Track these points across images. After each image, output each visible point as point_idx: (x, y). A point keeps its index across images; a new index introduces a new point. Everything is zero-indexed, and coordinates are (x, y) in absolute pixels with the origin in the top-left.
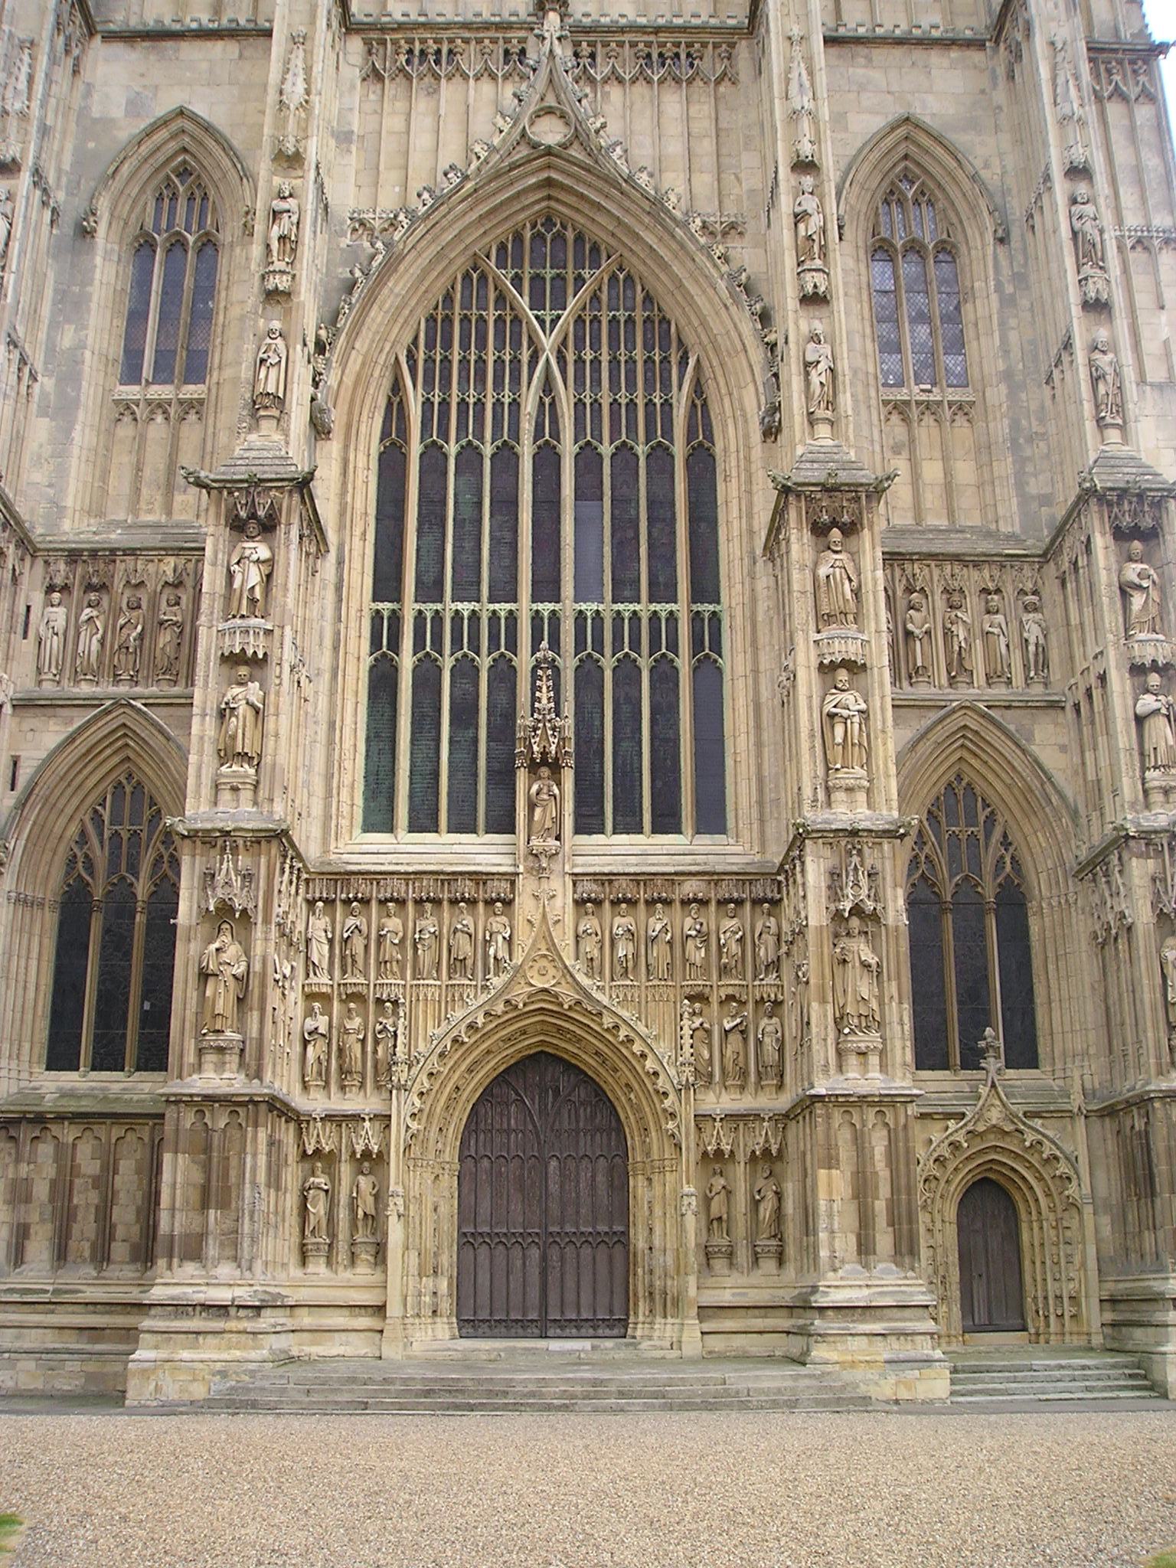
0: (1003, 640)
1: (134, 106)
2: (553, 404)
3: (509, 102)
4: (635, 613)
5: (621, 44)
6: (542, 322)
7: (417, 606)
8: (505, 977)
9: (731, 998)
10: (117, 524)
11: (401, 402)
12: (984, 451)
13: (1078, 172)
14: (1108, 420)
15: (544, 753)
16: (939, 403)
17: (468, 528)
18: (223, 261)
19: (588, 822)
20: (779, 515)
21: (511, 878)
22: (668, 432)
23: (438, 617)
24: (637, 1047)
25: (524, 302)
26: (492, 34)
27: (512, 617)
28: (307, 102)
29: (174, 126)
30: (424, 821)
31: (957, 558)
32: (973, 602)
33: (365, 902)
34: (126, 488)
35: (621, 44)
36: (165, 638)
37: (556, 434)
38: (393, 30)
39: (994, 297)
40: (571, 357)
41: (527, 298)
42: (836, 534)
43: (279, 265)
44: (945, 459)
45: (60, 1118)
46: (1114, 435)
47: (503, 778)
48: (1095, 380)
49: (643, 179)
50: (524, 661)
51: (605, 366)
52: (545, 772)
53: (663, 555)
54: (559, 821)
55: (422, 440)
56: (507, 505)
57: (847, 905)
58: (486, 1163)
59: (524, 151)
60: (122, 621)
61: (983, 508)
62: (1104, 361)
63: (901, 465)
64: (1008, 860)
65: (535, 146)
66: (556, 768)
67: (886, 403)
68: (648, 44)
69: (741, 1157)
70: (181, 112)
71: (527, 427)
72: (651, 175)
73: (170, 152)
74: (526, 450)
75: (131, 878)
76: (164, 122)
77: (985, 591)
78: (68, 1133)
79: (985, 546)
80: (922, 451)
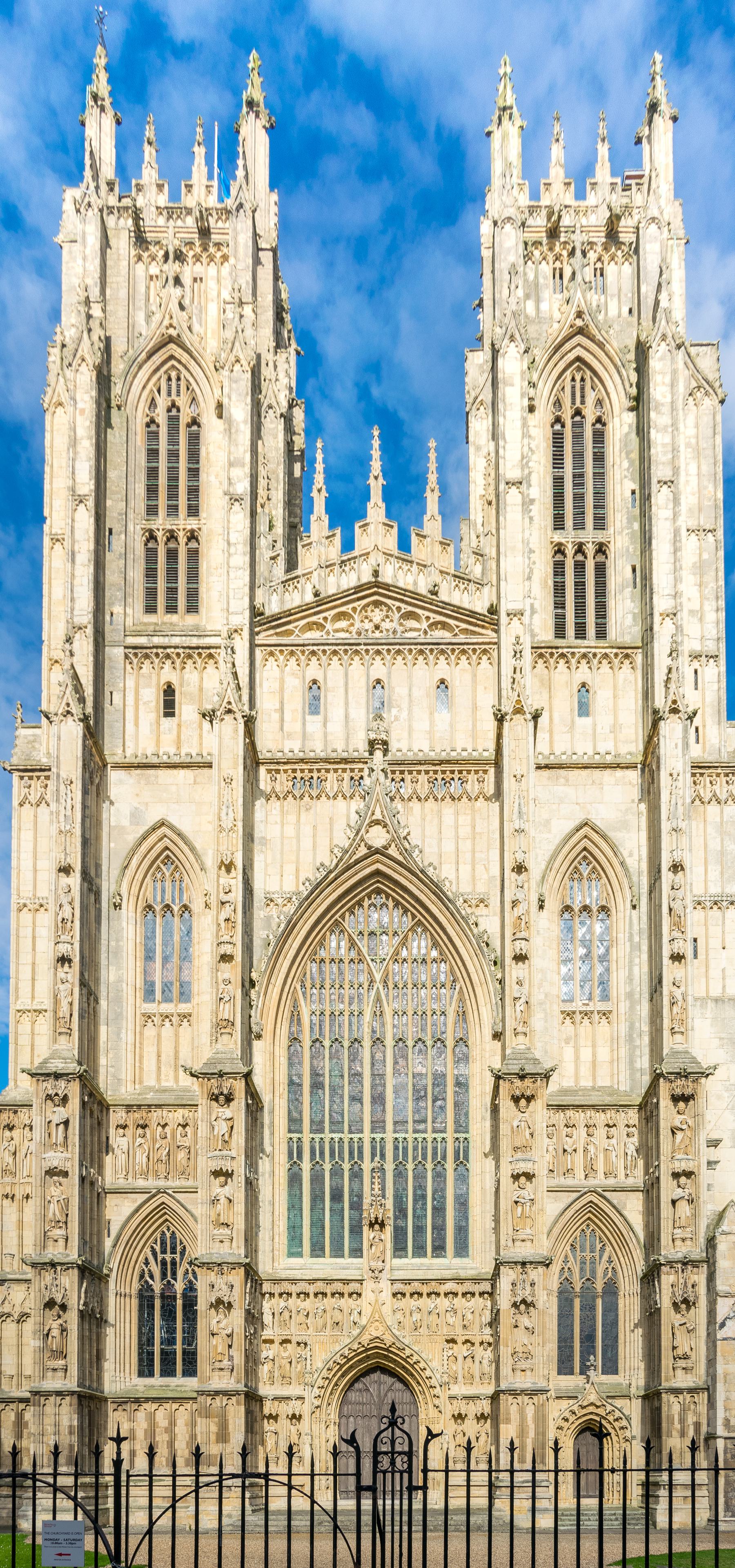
0: (614, 1154)
1: (136, 816)
3: (354, 817)
5: (419, 772)
8: (358, 1331)
9: (467, 1341)
12: (614, 1040)
14: (676, 1029)
15: (376, 1219)
18: (195, 918)
19: (399, 1249)
20: (496, 1088)
21: (361, 1282)
24: (422, 1365)
29: (159, 832)
30: (317, 1250)
31: (593, 1107)
32: (600, 1133)
33: (289, 1294)
34: (154, 1068)
35: (419, 772)
36: (181, 1155)
38: (284, 763)
39: (628, 944)
44: (594, 1046)
45: (147, 1400)
47: (357, 1230)
49: (430, 871)
50: (367, 1166)
52: (377, 1227)
54: (383, 1252)
57: (519, 1299)
58: (351, 1419)
59: (363, 851)
60: (157, 1146)
61: (612, 1076)
62: (678, 993)
63: (569, 1052)
64: (610, 1270)
65: (369, 848)
66: (382, 1225)
67: (563, 1012)
68: (435, 772)
69: (471, 1416)
70: (162, 824)
72: (435, 869)
73: (159, 851)
75: (173, 1282)
76: (154, 829)
77: (608, 1126)
78: (151, 1407)
79: (608, 1100)
80: (582, 1042)
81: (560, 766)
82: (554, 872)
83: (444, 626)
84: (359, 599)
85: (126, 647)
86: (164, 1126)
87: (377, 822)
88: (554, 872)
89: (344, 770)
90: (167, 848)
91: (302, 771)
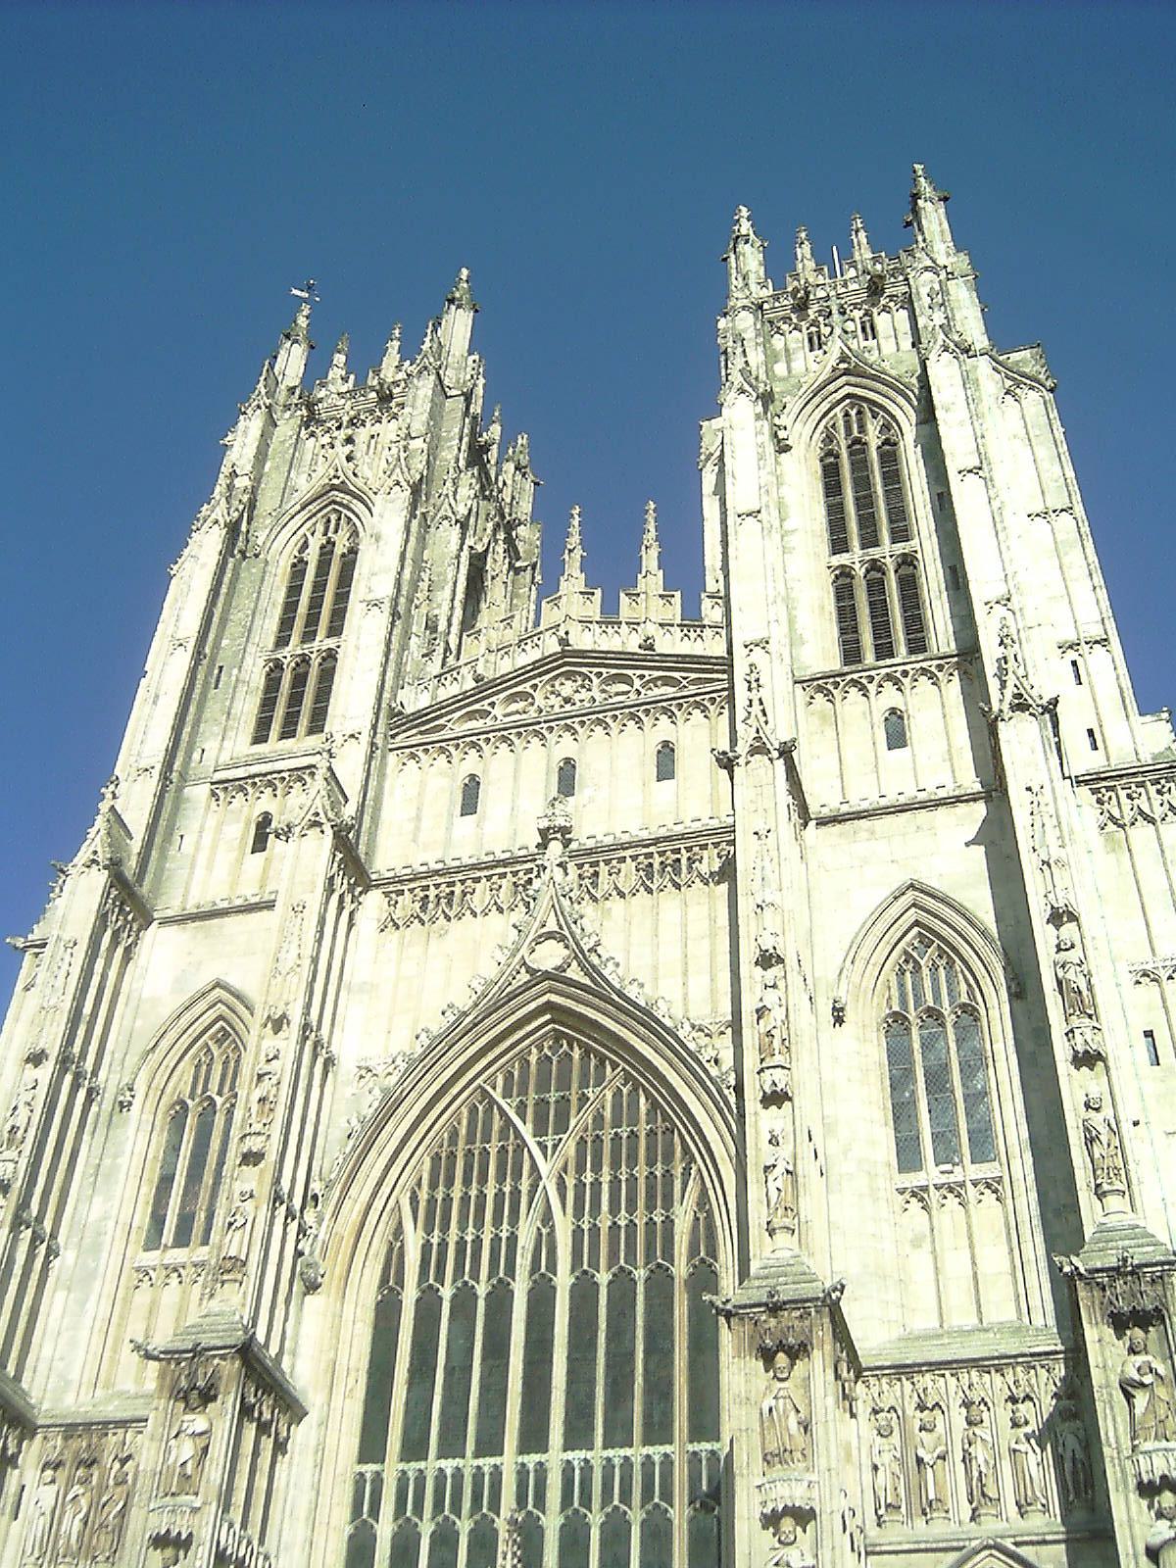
2: (552, 1234)
4: (626, 1458)
6: (543, 1148)
7: (402, 1466)
10: (120, 1394)
11: (402, 1247)
13: (1059, 917)
16: (962, 1185)
17: (458, 1373)
22: (668, 1254)
23: (421, 1477)
25: (526, 1130)
26: (501, 870)
27: (497, 1472)
28: (299, 966)
31: (974, 1363)
35: (622, 860)
37: (552, 1266)
38: (410, 880)
40: (570, 1182)
41: (530, 1125)
42: (781, 1359)
43: (257, 1127)
46: (1113, 1202)
48: (1091, 1140)
51: (605, 1187)
53: (659, 1390)
55: (454, 1281)
56: (497, 1349)
59: (524, 977)
70: (218, 985)
71: (523, 1262)
74: (521, 1288)
81: (859, 816)
82: (860, 964)
83: (668, 681)
84: (540, 675)
85: (212, 783)
86: (124, 1462)
87: (550, 936)
88: (860, 964)
89: (503, 876)
90: (220, 1018)
91: (437, 886)
